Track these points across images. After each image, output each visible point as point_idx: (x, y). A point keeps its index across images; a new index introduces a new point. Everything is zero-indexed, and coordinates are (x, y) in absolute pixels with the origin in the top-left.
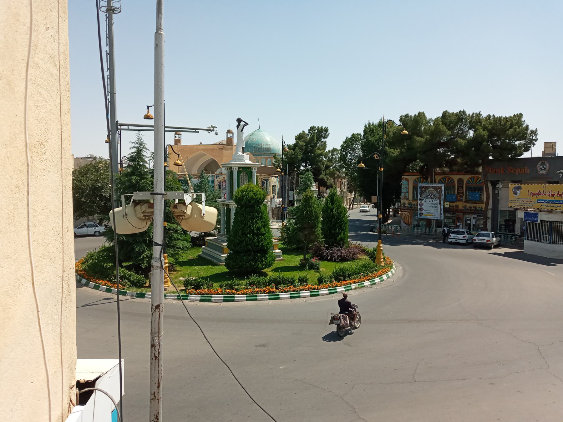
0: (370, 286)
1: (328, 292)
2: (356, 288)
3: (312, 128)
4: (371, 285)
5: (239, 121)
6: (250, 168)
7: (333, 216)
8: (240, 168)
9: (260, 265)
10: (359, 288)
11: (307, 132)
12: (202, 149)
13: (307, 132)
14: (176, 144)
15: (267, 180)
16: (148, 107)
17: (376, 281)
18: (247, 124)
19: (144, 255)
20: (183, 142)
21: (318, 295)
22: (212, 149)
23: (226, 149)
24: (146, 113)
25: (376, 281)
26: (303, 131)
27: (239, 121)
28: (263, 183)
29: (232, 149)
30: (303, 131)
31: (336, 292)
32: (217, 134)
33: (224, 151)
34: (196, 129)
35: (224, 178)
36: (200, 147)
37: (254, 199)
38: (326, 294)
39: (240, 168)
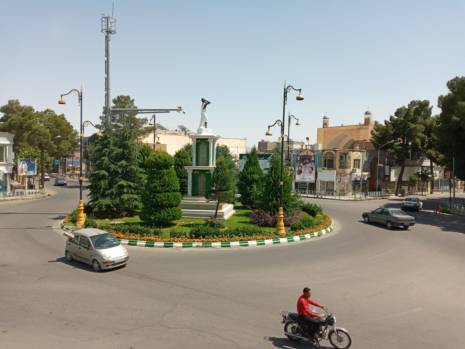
0: (220, 247)
1: (163, 245)
2: (197, 246)
3: (413, 103)
4: (222, 246)
5: (203, 101)
6: (208, 139)
7: (270, 183)
8: (197, 139)
9: (152, 218)
10: (202, 247)
11: (407, 107)
12: (343, 130)
13: (407, 107)
14: (324, 127)
15: (346, 154)
16: (62, 95)
17: (231, 244)
18: (209, 103)
19: (97, 202)
20: (330, 125)
21: (153, 246)
22: (351, 130)
23: (363, 129)
24: (60, 100)
25: (231, 244)
26: (404, 107)
27: (203, 101)
28: (341, 157)
29: (368, 128)
30: (404, 107)
31: (172, 247)
32: (184, 113)
33: (361, 131)
34: (167, 110)
35: (307, 152)
36: (341, 128)
37: (154, 162)
38: (161, 247)
39: (197, 139)
